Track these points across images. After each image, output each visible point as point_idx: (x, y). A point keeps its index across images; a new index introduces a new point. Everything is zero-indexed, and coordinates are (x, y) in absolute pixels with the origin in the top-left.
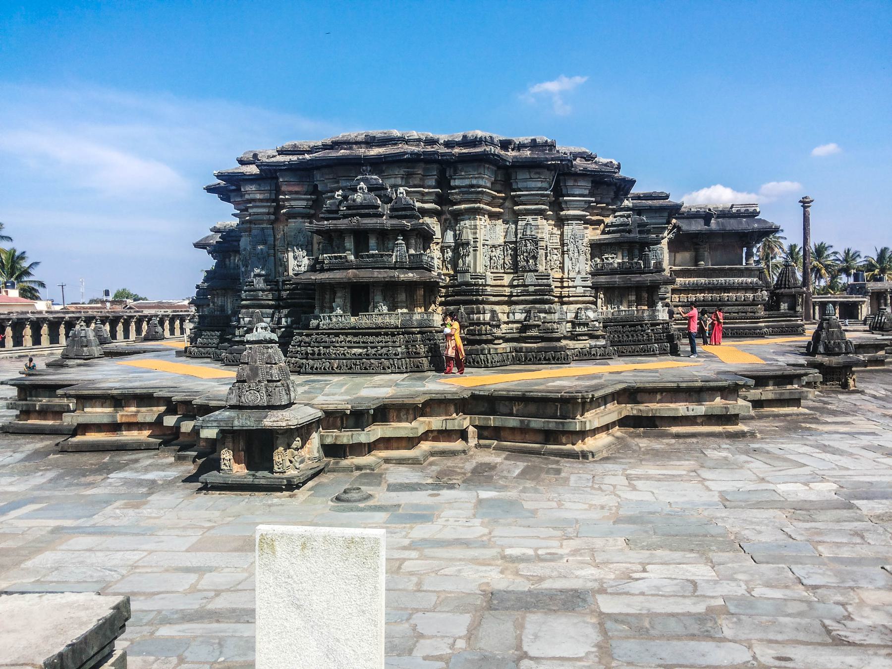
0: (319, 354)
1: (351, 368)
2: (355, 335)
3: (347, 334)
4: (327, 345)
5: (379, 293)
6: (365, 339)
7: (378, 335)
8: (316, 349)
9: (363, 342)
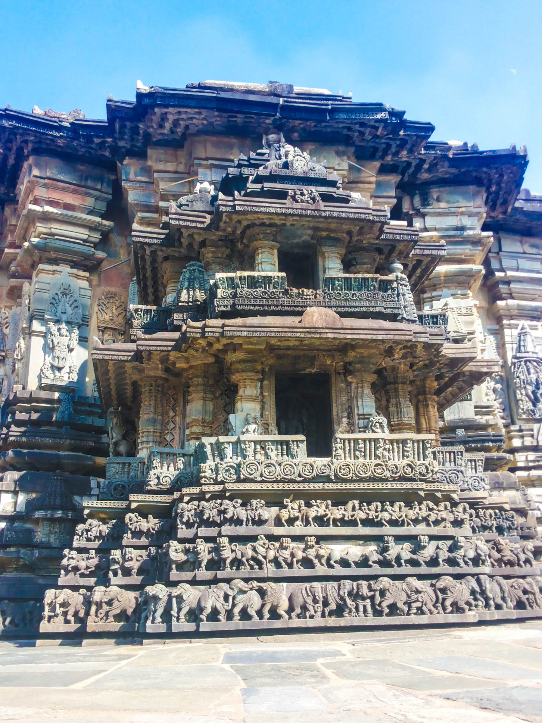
0: (216, 564)
1: (339, 611)
2: (339, 499)
3: (308, 498)
4: (242, 530)
5: (367, 391)
6: (372, 511)
7: (410, 499)
8: (203, 548)
9: (368, 522)
